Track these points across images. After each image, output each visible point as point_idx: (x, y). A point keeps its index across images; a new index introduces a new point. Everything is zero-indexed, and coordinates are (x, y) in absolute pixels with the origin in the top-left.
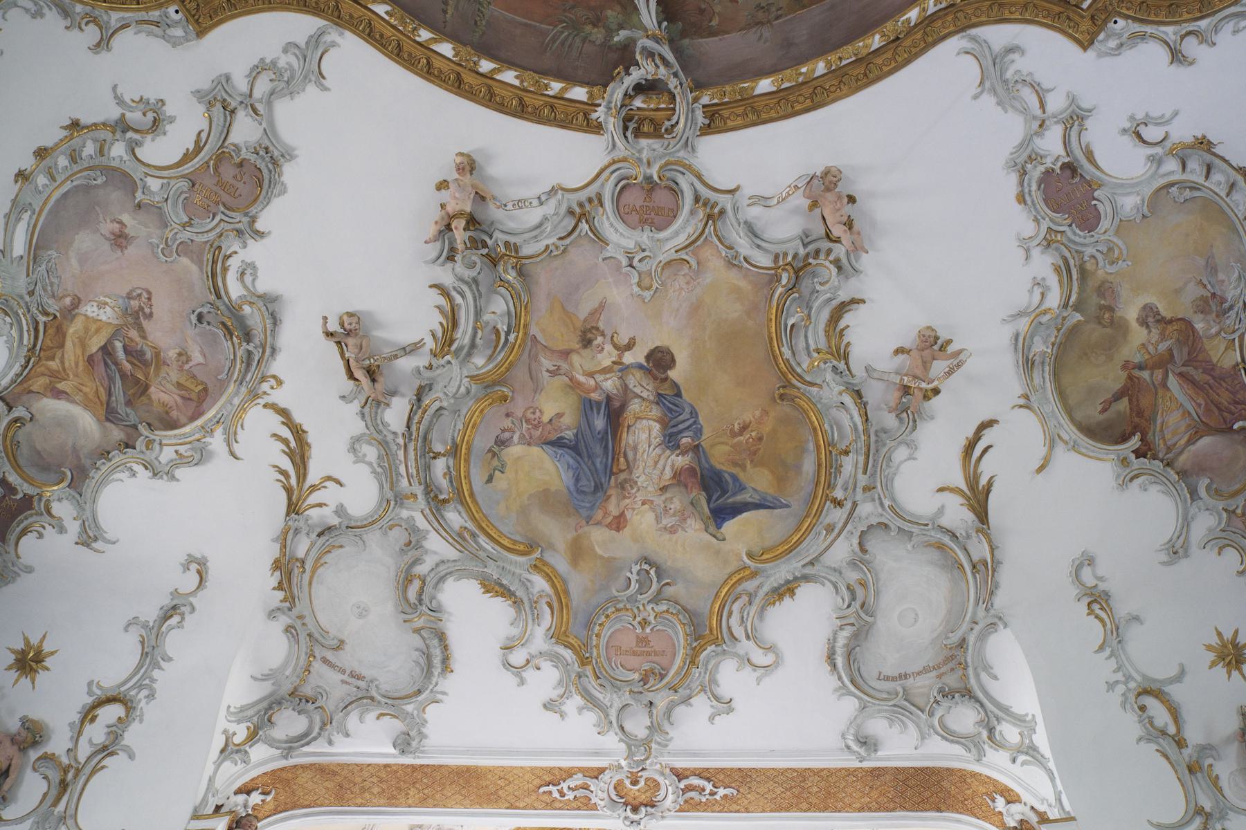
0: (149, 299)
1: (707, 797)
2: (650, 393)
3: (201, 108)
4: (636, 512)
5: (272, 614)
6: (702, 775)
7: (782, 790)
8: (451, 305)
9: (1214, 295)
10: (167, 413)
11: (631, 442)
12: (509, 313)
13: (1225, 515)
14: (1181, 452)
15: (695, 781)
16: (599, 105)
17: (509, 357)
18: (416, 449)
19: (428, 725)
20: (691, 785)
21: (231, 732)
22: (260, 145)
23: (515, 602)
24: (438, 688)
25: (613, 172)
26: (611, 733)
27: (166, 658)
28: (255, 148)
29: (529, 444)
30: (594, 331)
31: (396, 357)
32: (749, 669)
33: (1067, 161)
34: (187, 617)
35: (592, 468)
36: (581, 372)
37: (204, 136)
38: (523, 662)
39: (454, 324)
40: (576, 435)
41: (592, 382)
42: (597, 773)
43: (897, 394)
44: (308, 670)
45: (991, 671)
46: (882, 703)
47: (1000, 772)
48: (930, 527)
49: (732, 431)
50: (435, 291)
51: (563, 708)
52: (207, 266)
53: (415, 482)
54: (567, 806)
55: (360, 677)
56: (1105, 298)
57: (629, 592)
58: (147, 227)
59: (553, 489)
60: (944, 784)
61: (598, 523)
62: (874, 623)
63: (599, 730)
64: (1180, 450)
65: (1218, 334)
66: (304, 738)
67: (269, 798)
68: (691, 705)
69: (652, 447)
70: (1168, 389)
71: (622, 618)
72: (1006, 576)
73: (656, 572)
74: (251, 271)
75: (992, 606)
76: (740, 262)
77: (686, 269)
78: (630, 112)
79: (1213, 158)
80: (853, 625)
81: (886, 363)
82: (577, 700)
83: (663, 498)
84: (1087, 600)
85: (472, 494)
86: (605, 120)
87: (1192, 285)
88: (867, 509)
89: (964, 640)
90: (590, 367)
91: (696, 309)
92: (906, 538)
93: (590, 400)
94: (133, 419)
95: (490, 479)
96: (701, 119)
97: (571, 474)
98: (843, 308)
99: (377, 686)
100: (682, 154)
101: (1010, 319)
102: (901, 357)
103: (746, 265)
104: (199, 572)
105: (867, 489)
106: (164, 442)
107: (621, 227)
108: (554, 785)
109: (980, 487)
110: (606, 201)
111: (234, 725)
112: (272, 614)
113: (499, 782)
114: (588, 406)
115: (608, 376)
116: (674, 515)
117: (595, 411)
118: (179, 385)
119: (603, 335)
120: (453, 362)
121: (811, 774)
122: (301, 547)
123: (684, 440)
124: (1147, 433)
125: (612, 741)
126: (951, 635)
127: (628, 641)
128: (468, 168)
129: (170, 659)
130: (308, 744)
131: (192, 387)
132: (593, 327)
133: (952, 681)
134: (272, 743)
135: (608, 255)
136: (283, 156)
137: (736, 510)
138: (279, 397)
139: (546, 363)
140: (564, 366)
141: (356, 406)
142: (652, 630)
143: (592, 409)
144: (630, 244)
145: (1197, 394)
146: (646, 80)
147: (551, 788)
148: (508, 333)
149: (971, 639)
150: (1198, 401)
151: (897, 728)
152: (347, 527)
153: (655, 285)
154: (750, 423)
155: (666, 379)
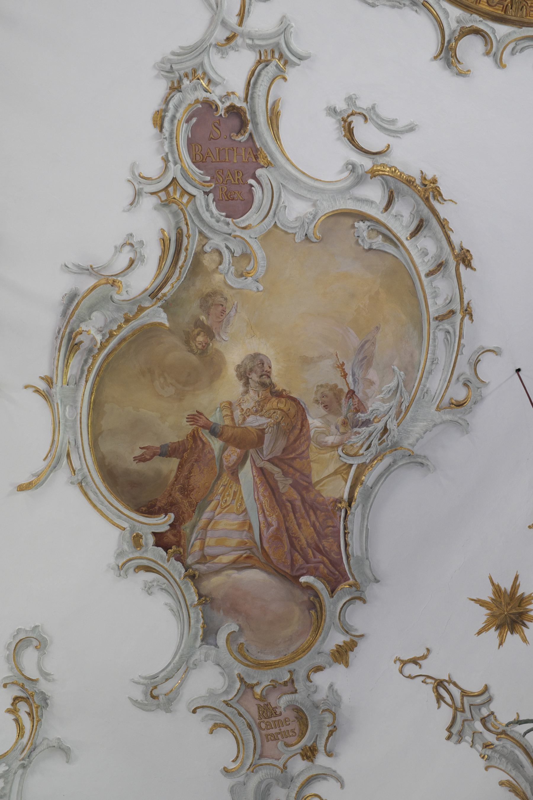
9: (352, 393)
13: (238, 685)
14: (218, 572)
33: (238, 105)
64: (220, 566)
65: (334, 447)
70: (237, 480)
79: (431, 215)
84: (16, 692)
87: (327, 364)
101: (75, 269)
124: (184, 521)
150: (270, 519)
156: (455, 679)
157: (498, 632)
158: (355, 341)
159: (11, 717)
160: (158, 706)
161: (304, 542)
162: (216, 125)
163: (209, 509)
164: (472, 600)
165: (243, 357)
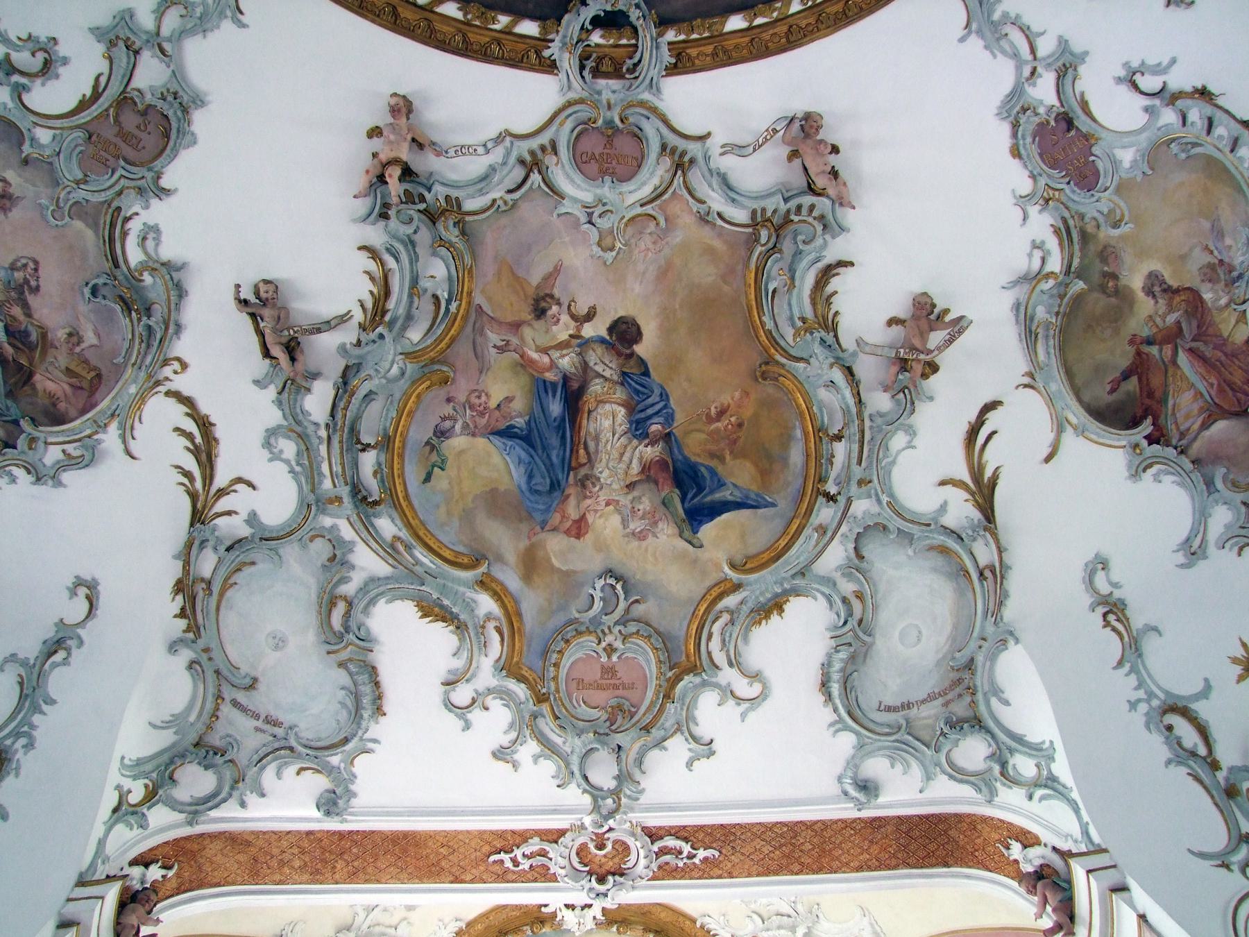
0: (36, 270)
1: (685, 860)
2: (613, 372)
3: (100, 48)
4: (598, 515)
5: (173, 647)
6: (678, 835)
7: (771, 849)
8: (383, 270)
9: (1221, 261)
10: (54, 405)
11: (592, 430)
12: (450, 278)
13: (1243, 509)
15: (670, 842)
16: (552, 41)
17: (450, 330)
18: (341, 442)
19: (357, 781)
20: (666, 847)
21: (125, 789)
22: (168, 90)
23: (458, 628)
24: (367, 736)
25: (570, 115)
26: (573, 786)
27: (49, 701)
28: (162, 94)
29: (474, 435)
30: (549, 300)
31: (319, 331)
32: (731, 702)
34: (74, 652)
35: (547, 461)
36: (534, 348)
37: (103, 80)
38: (467, 701)
39: (387, 293)
40: (528, 423)
41: (546, 360)
42: (554, 836)
43: (895, 369)
44: (215, 715)
46: (883, 738)
47: (1014, 812)
48: (932, 527)
49: (708, 416)
50: (365, 254)
51: (516, 757)
52: (104, 229)
53: (340, 481)
54: (522, 877)
55: (276, 723)
56: (1108, 264)
57: (592, 613)
58: (34, 185)
59: (502, 488)
60: (952, 833)
61: (554, 529)
62: (873, 644)
63: (558, 782)
65: (1227, 305)
66: (212, 800)
67: (171, 873)
68: (666, 749)
69: (617, 436)
70: (1178, 367)
71: (585, 644)
72: (1014, 583)
73: (623, 588)
74: (155, 235)
75: (1002, 619)
76: (714, 219)
77: (652, 225)
78: (587, 49)
80: (850, 644)
81: (877, 334)
82: (531, 747)
83: (630, 497)
84: (1101, 610)
85: (407, 497)
86: (560, 57)
87: (1197, 252)
88: (861, 506)
89: (972, 660)
90: (544, 341)
91: (664, 272)
92: (907, 541)
93: (545, 381)
94: (14, 412)
95: (428, 479)
96: (668, 59)
97: (522, 470)
98: (828, 272)
99: (296, 734)
100: (646, 96)
102: (896, 330)
103: (719, 222)
104: (88, 597)
105: (861, 483)
106: (50, 440)
107: (578, 178)
108: (506, 852)
110: (561, 148)
111: (130, 780)
112: (173, 647)
113: (442, 850)
114: (542, 388)
115: (564, 352)
116: (642, 518)
117: (550, 394)
118: (69, 372)
119: (559, 304)
120: (385, 333)
121: (803, 828)
122: (206, 564)
123: (654, 428)
124: (1159, 416)
125: (575, 796)
126: (958, 655)
127: (594, 674)
128: (404, 110)
129: (53, 702)
130: (216, 806)
131: (84, 373)
132: (547, 295)
133: (960, 709)
134: (174, 805)
135: (564, 210)
136: (194, 102)
137: (715, 510)
138: (182, 383)
139: (494, 337)
140: (515, 341)
141: (272, 391)
142: (619, 658)
143: (546, 392)
144: (588, 197)
145: (1208, 372)
146: (604, 11)
147: (502, 856)
148: (449, 302)
149: (980, 659)
151: (899, 767)
152: (261, 539)
153: (618, 245)
154: (729, 406)
155: (632, 355)
158: (1206, 225)
159: (1109, 629)
160: (1198, 559)
161: (1239, 383)
163: (1170, 397)
165: (1143, 279)
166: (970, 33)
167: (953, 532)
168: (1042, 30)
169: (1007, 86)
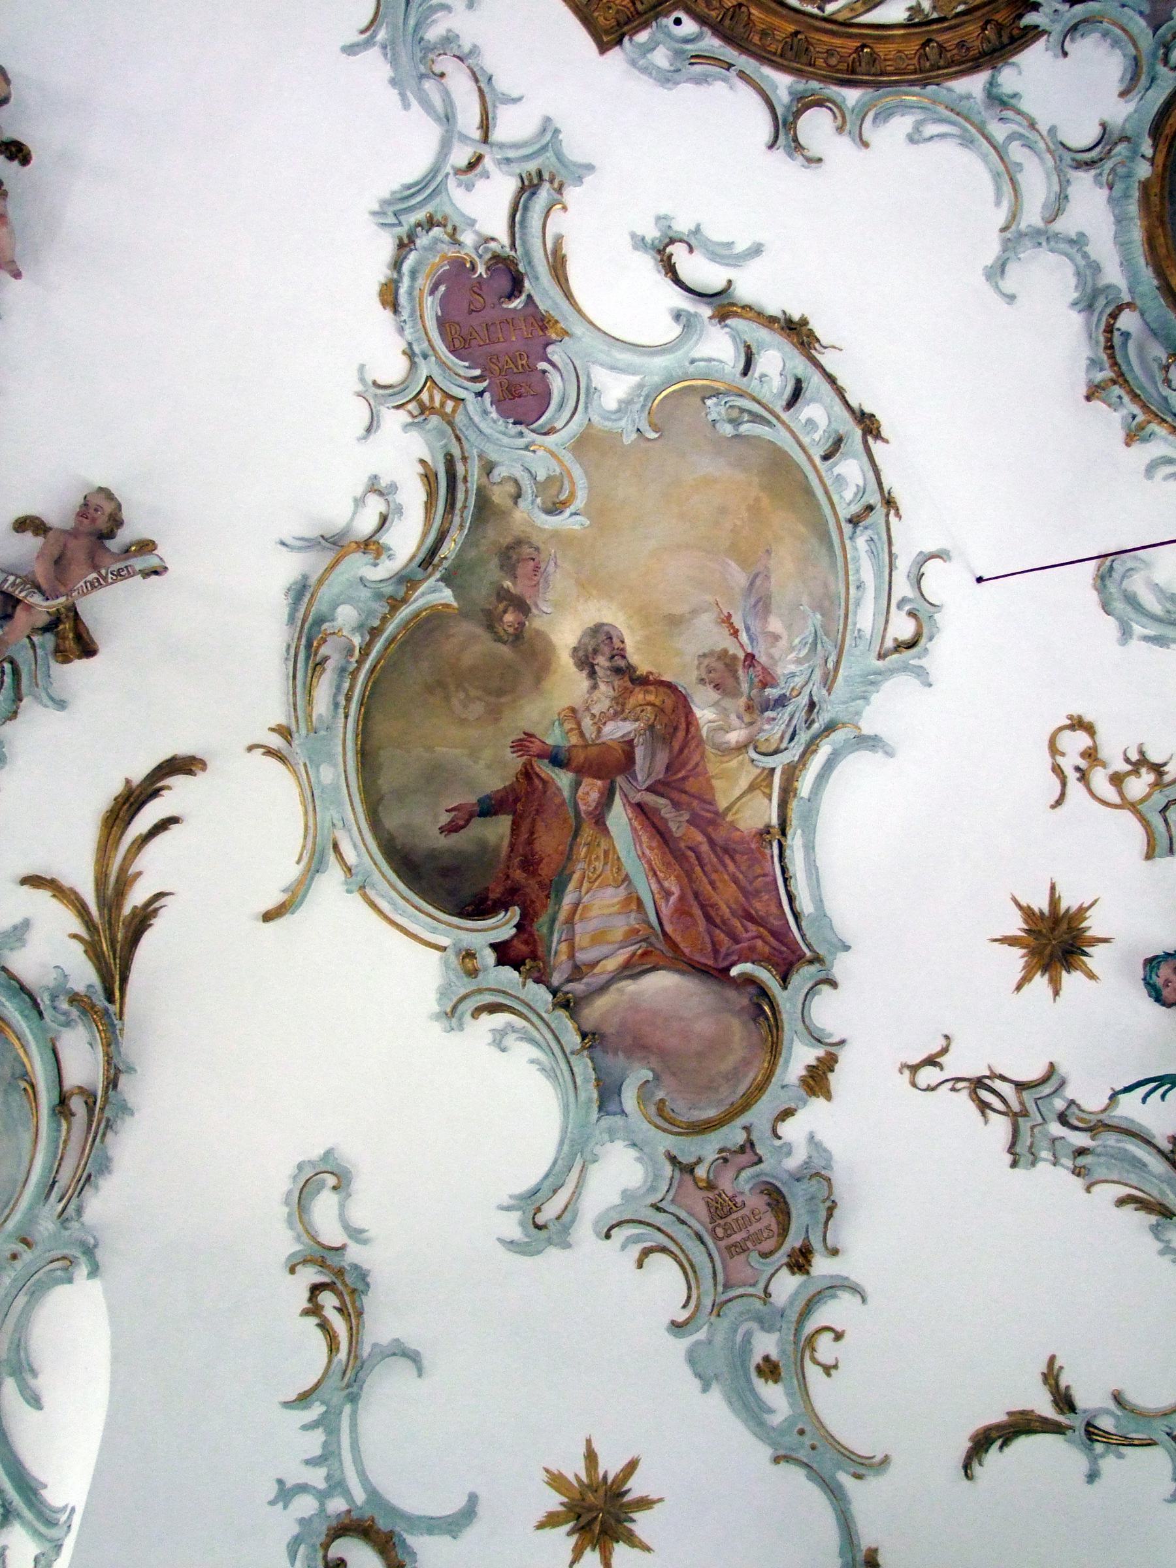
9: (750, 658)
13: (668, 1169)
14: (603, 989)
45: (32, 1382)
56: (514, 577)
64: (604, 978)
65: (742, 748)
70: (605, 831)
75: (79, 1211)
79: (811, 369)
84: (311, 1275)
87: (706, 620)
102: (31, 543)
109: (127, 910)
124: (537, 915)
145: (668, 865)
150: (666, 884)
156: (999, 1070)
157: (1047, 976)
158: (739, 578)
159: (313, 1321)
160: (550, 1242)
161: (724, 909)
162: (475, 289)
163: (571, 886)
164: (996, 940)
165: (579, 633)
166: (368, 43)
167: (23, 988)
168: (515, 95)
169: (415, 167)
